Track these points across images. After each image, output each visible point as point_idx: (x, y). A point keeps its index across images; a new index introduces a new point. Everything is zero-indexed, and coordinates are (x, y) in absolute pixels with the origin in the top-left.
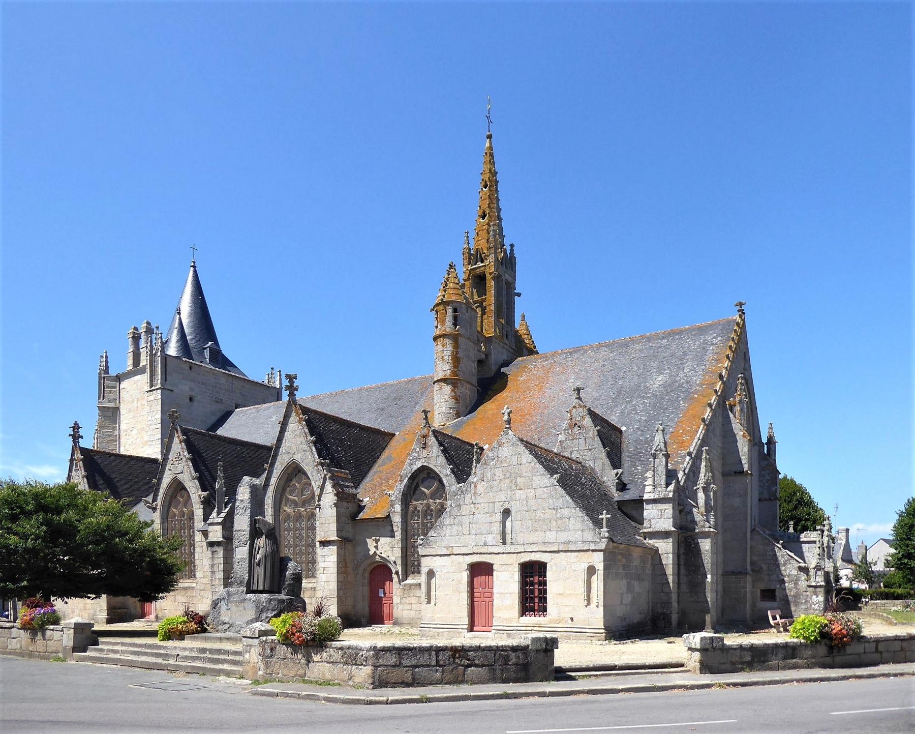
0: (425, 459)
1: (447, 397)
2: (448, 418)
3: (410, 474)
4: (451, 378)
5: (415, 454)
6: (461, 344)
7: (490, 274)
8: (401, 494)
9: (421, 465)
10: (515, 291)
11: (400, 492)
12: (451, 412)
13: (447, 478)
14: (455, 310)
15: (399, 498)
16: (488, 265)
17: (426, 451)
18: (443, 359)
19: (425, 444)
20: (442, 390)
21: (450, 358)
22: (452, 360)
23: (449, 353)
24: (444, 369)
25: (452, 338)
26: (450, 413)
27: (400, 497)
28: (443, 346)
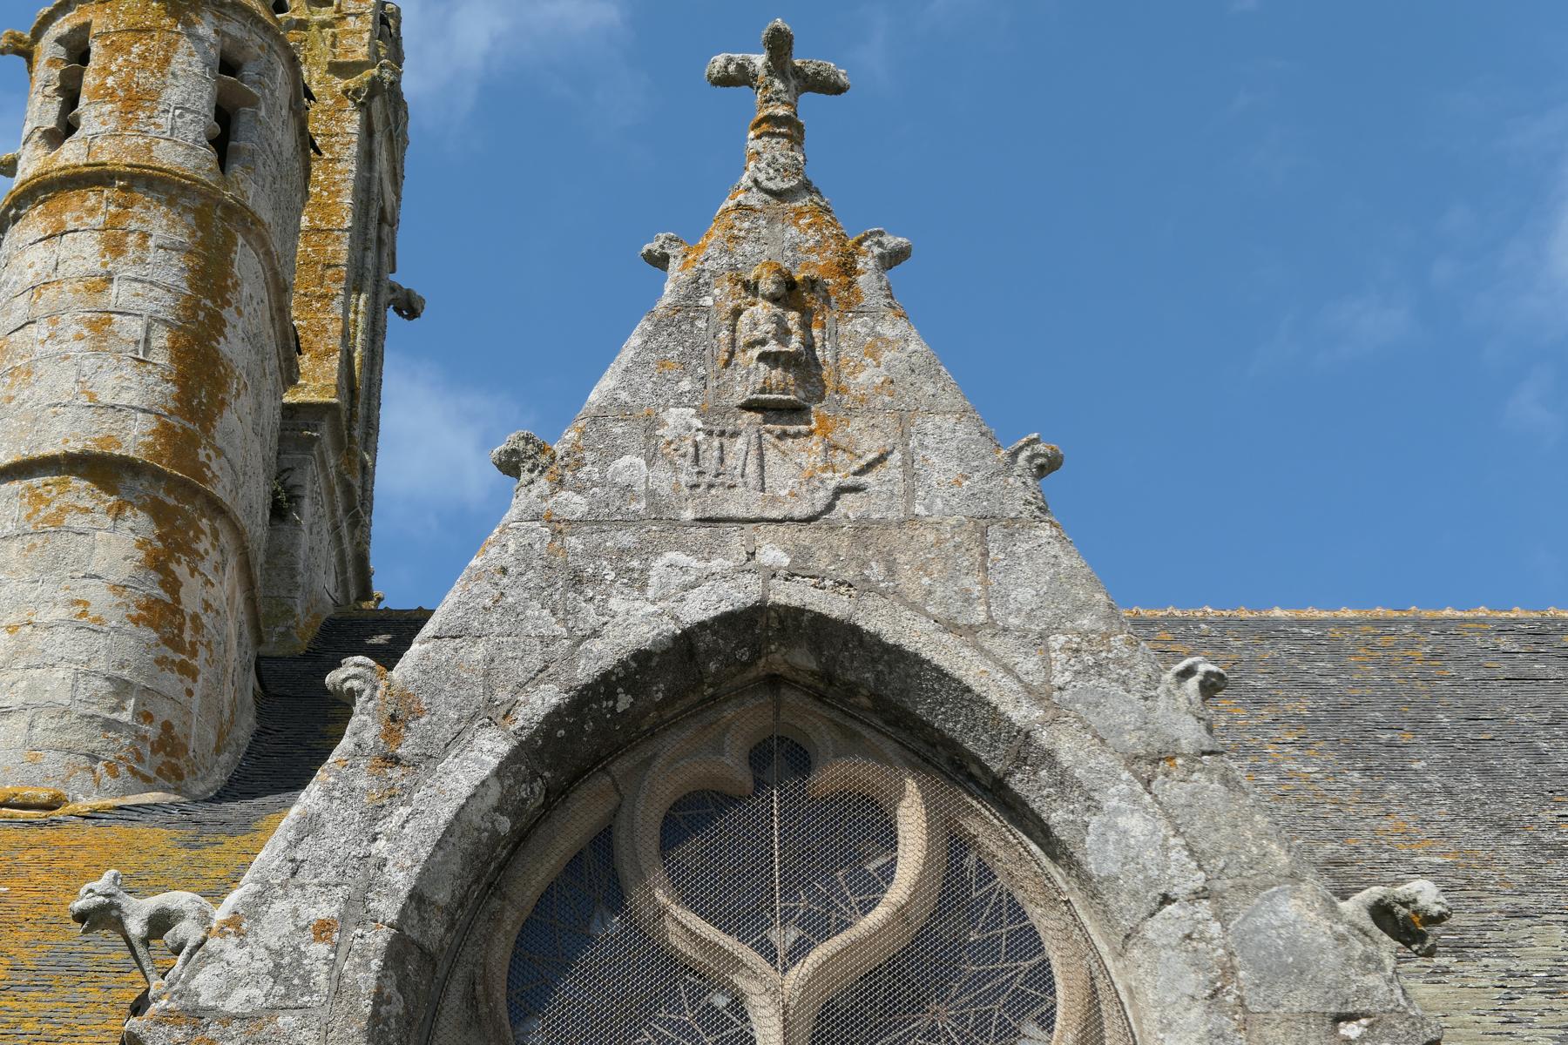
0: (806, 536)
1: (99, 597)
2: (93, 757)
3: (545, 699)
4: (158, 475)
5: (629, 466)
6: (246, 290)
7: (339, 69)
8: (379, 938)
9: (738, 594)
10: (392, 277)
11: (356, 909)
12: (126, 717)
13: (1173, 790)
14: (228, 66)
15: (338, 990)
16: (323, 25)
17: (809, 453)
18: (100, 325)
19: (803, 365)
20: (60, 541)
21: (161, 339)
22: (179, 353)
23: (161, 303)
24: (106, 398)
25: (190, 218)
26: (109, 725)
27: (365, 978)
28: (115, 247)
